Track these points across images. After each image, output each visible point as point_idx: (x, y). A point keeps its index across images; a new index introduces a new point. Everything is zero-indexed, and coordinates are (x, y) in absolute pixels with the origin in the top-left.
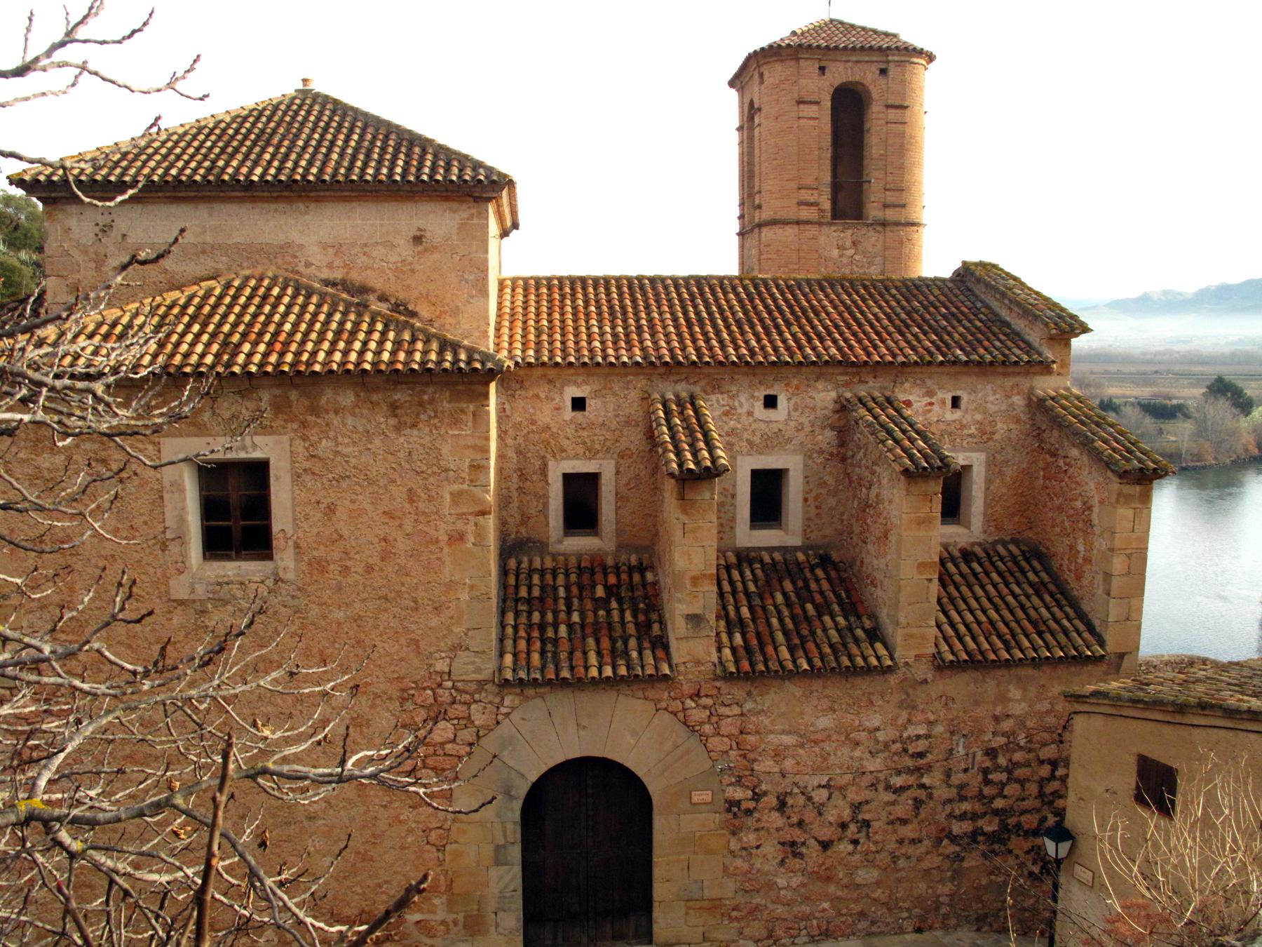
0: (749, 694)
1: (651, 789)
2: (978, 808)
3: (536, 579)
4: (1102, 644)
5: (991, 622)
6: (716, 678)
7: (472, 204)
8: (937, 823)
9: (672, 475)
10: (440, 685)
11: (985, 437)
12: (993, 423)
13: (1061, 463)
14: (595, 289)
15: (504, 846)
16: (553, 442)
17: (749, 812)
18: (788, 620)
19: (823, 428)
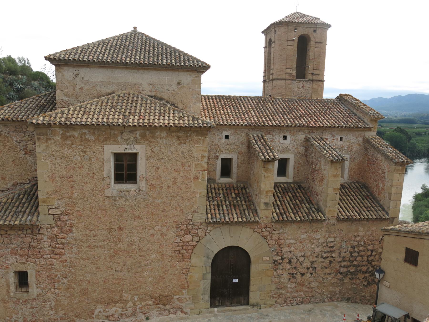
0: (281, 227)
1: (251, 256)
2: (349, 264)
3: (213, 191)
4: (388, 215)
5: (353, 207)
6: (272, 222)
7: (196, 73)
8: (336, 268)
9: (262, 160)
10: (189, 223)
11: (349, 150)
12: (352, 146)
13: (374, 159)
14: (227, 100)
15: (206, 274)
16: (218, 149)
17: (280, 264)
18: (292, 205)
19: (301, 146)
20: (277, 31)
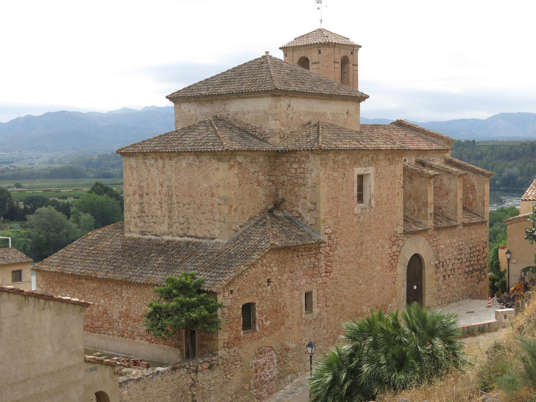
20: (322, 51)
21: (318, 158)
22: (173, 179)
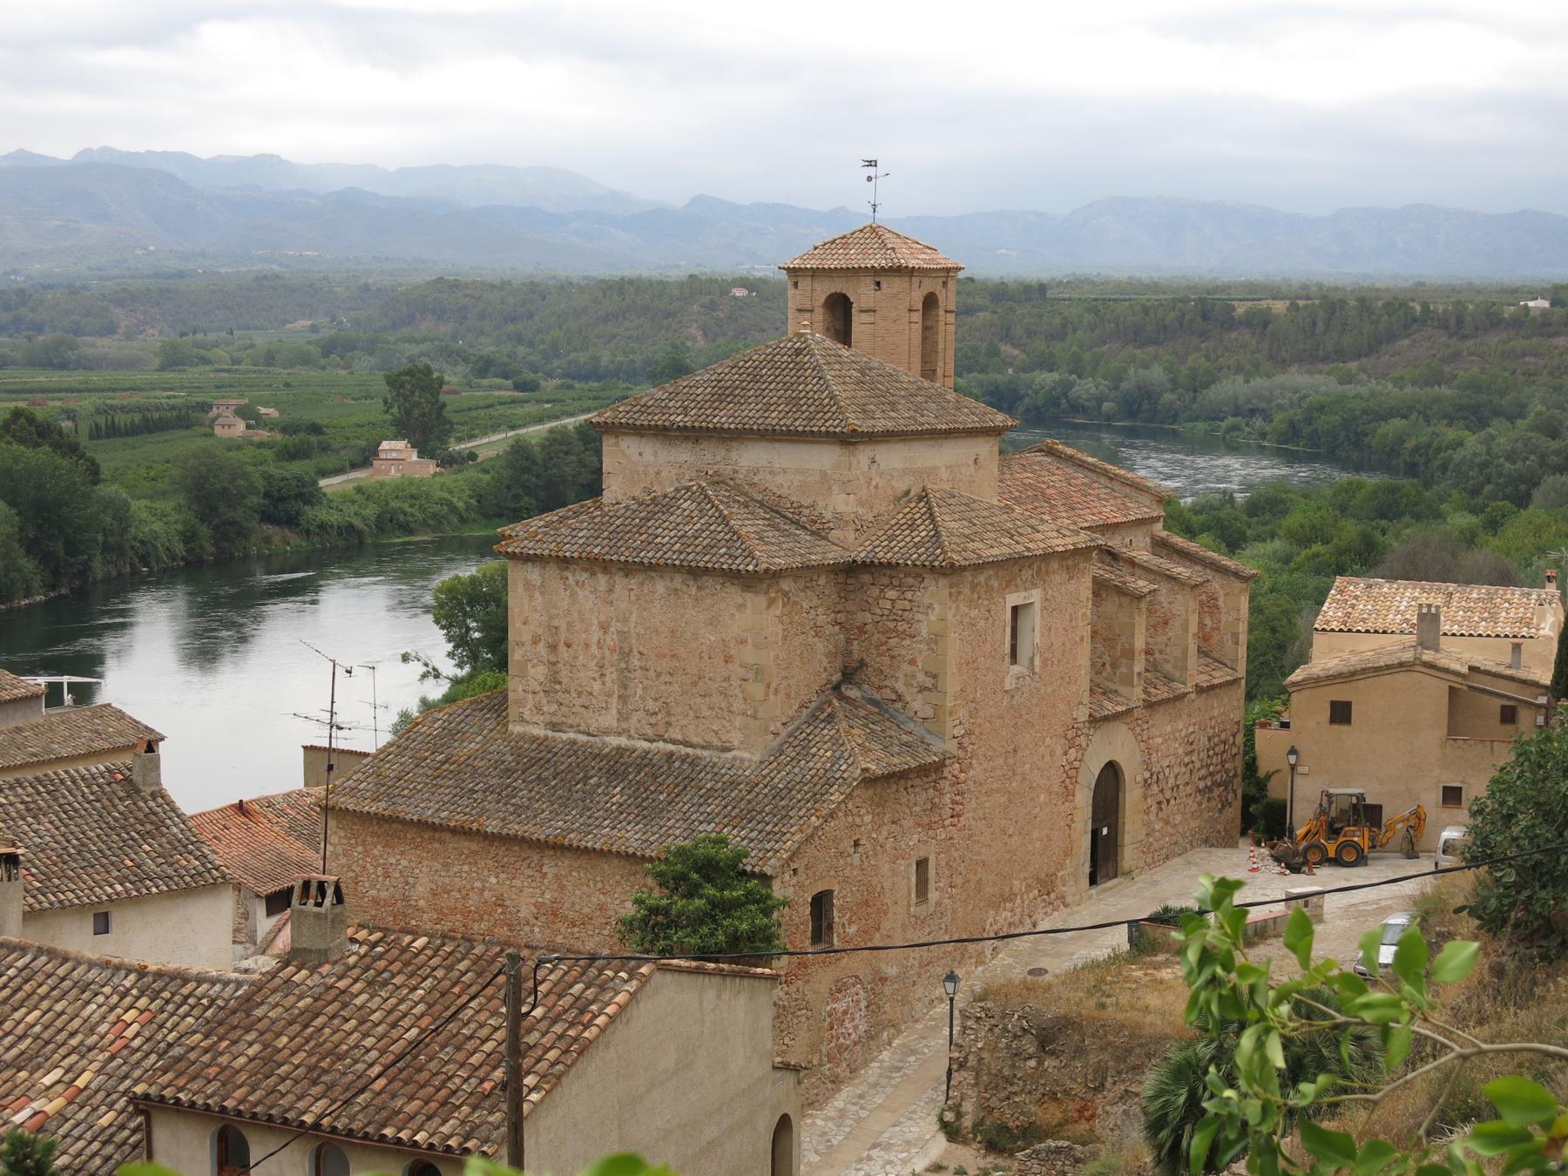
20: (884, 285)
21: (943, 582)
22: (634, 618)
